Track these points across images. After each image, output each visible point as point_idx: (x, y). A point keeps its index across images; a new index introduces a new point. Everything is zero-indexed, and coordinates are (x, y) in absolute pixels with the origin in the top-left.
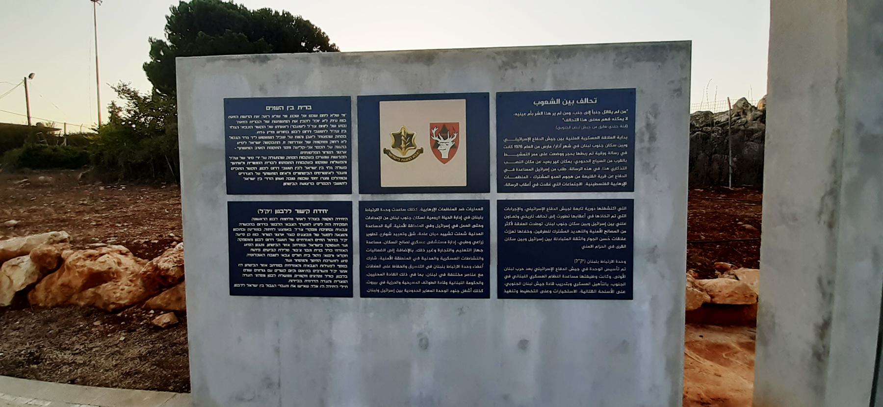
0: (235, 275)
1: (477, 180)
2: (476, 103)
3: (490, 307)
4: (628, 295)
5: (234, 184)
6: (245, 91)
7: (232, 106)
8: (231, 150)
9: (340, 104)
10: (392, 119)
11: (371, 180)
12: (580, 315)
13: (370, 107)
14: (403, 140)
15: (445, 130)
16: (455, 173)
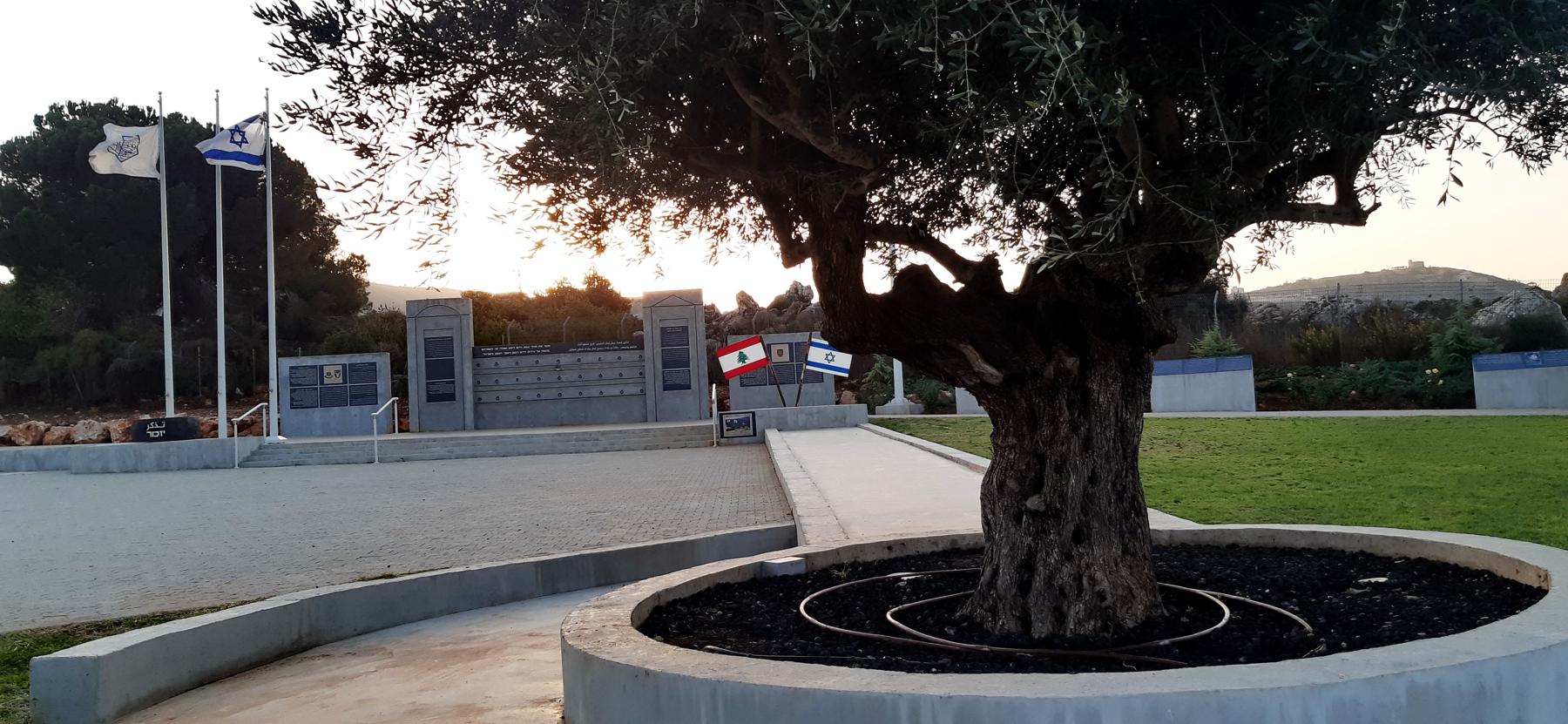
2: (344, 366)
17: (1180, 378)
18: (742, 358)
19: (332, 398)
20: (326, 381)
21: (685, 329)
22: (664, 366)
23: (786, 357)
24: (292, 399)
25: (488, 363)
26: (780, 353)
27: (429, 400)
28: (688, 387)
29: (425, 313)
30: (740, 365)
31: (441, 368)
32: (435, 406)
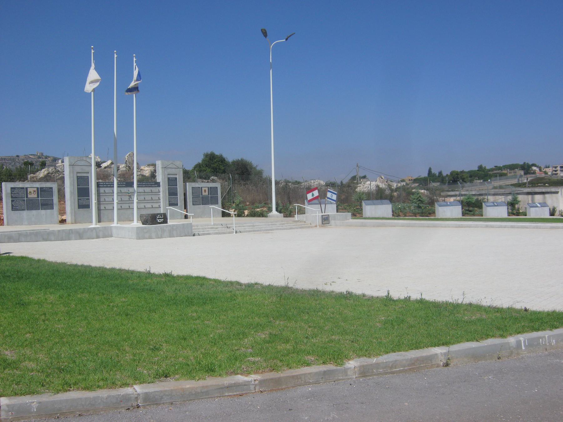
0: (12, 208)
1: (38, 197)
2: (38, 188)
3: (40, 211)
4: (53, 209)
5: (12, 197)
6: (13, 186)
7: (12, 188)
8: (11, 193)
9: (23, 188)
10: (29, 190)
11: (27, 197)
12: (49, 211)
13: (27, 188)
14: (30, 192)
15: (35, 191)
16: (36, 196)
17: (374, 206)
18: (313, 195)
19: (32, 205)
20: (29, 196)
21: (176, 178)
22: (170, 194)
23: (207, 193)
24: (12, 206)
25: (102, 190)
26: (205, 191)
27: (79, 208)
28: (177, 205)
29: (79, 163)
30: (312, 198)
31: (83, 192)
32: (82, 210)
